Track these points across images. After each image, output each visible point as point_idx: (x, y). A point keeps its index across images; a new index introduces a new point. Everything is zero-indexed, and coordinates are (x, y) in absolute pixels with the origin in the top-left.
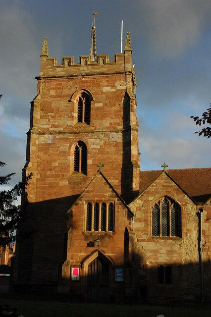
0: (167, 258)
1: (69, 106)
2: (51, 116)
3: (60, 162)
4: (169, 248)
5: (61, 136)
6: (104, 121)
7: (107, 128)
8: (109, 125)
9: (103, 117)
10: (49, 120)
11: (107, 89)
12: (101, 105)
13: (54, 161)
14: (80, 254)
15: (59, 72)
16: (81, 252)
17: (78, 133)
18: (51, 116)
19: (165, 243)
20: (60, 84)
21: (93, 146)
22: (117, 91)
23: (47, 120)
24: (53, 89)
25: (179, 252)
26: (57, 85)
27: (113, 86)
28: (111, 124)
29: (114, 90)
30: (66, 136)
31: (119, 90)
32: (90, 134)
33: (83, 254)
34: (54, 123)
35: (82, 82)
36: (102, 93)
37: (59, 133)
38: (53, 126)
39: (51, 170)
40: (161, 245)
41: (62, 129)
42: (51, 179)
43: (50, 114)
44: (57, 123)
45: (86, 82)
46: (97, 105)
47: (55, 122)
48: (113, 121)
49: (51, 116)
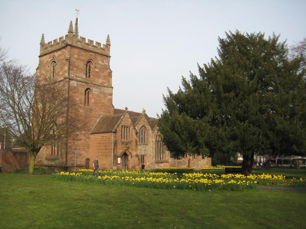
1: (84, 67)
4: (144, 148)
5: (81, 83)
7: (100, 84)
8: (101, 82)
9: (99, 77)
11: (100, 62)
12: (98, 70)
16: (120, 150)
18: (76, 70)
20: (80, 52)
27: (103, 62)
28: (102, 82)
32: (94, 86)
35: (90, 55)
37: (80, 82)
38: (76, 76)
43: (74, 69)
44: (78, 75)
45: (91, 55)
48: (103, 81)
49: (76, 70)
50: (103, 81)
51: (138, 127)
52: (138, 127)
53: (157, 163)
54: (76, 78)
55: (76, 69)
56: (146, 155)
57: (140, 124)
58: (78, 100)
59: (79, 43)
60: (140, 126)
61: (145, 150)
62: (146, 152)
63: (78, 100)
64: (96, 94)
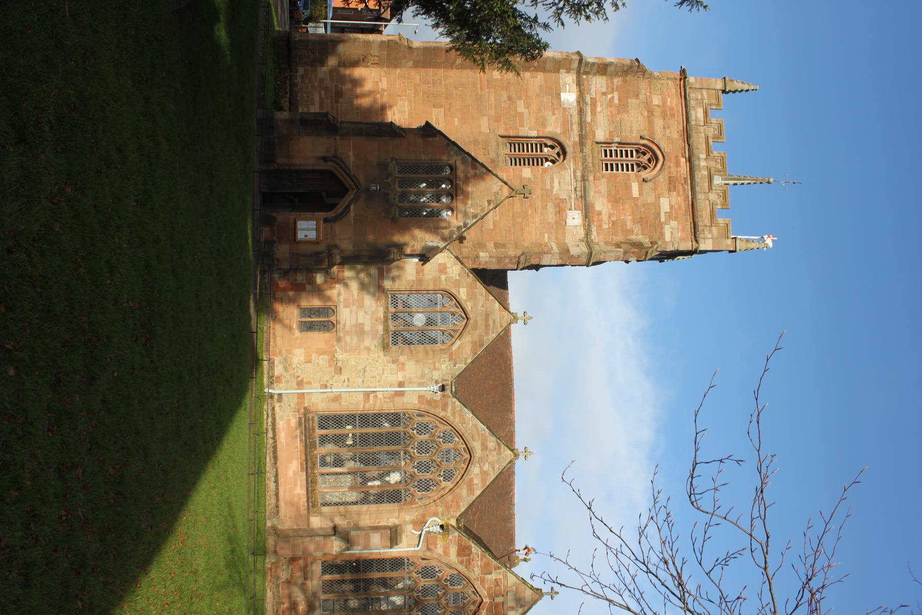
0: (348, 323)
1: (631, 131)
2: (613, 97)
3: (526, 116)
4: (367, 328)
6: (605, 201)
9: (615, 199)
10: (604, 94)
12: (635, 193)
13: (527, 106)
14: (351, 153)
15: (696, 113)
17: (582, 151)
18: (612, 99)
19: (377, 321)
20: (673, 116)
21: (556, 181)
22: (661, 226)
23: (604, 90)
24: (664, 102)
25: (362, 347)
26: (672, 109)
27: (669, 216)
28: (600, 213)
29: (663, 220)
30: (576, 128)
31: (662, 228)
33: (352, 159)
34: (599, 104)
35: (677, 157)
36: (658, 197)
39: (510, 98)
40: (373, 313)
41: (589, 119)
42: (492, 99)
43: (616, 95)
44: (599, 109)
45: (678, 164)
46: (635, 187)
47: (601, 105)
48: (605, 217)
49: (612, 99)
50: (605, 217)
51: (458, 284)
52: (458, 284)
53: (306, 420)
54: (588, 99)
55: (616, 101)
56: (339, 340)
57: (472, 296)
58: (519, 110)
59: (700, 113)
60: (462, 294)
61: (360, 331)
62: (355, 339)
63: (519, 110)
64: (552, 187)
